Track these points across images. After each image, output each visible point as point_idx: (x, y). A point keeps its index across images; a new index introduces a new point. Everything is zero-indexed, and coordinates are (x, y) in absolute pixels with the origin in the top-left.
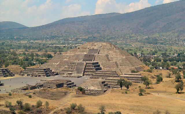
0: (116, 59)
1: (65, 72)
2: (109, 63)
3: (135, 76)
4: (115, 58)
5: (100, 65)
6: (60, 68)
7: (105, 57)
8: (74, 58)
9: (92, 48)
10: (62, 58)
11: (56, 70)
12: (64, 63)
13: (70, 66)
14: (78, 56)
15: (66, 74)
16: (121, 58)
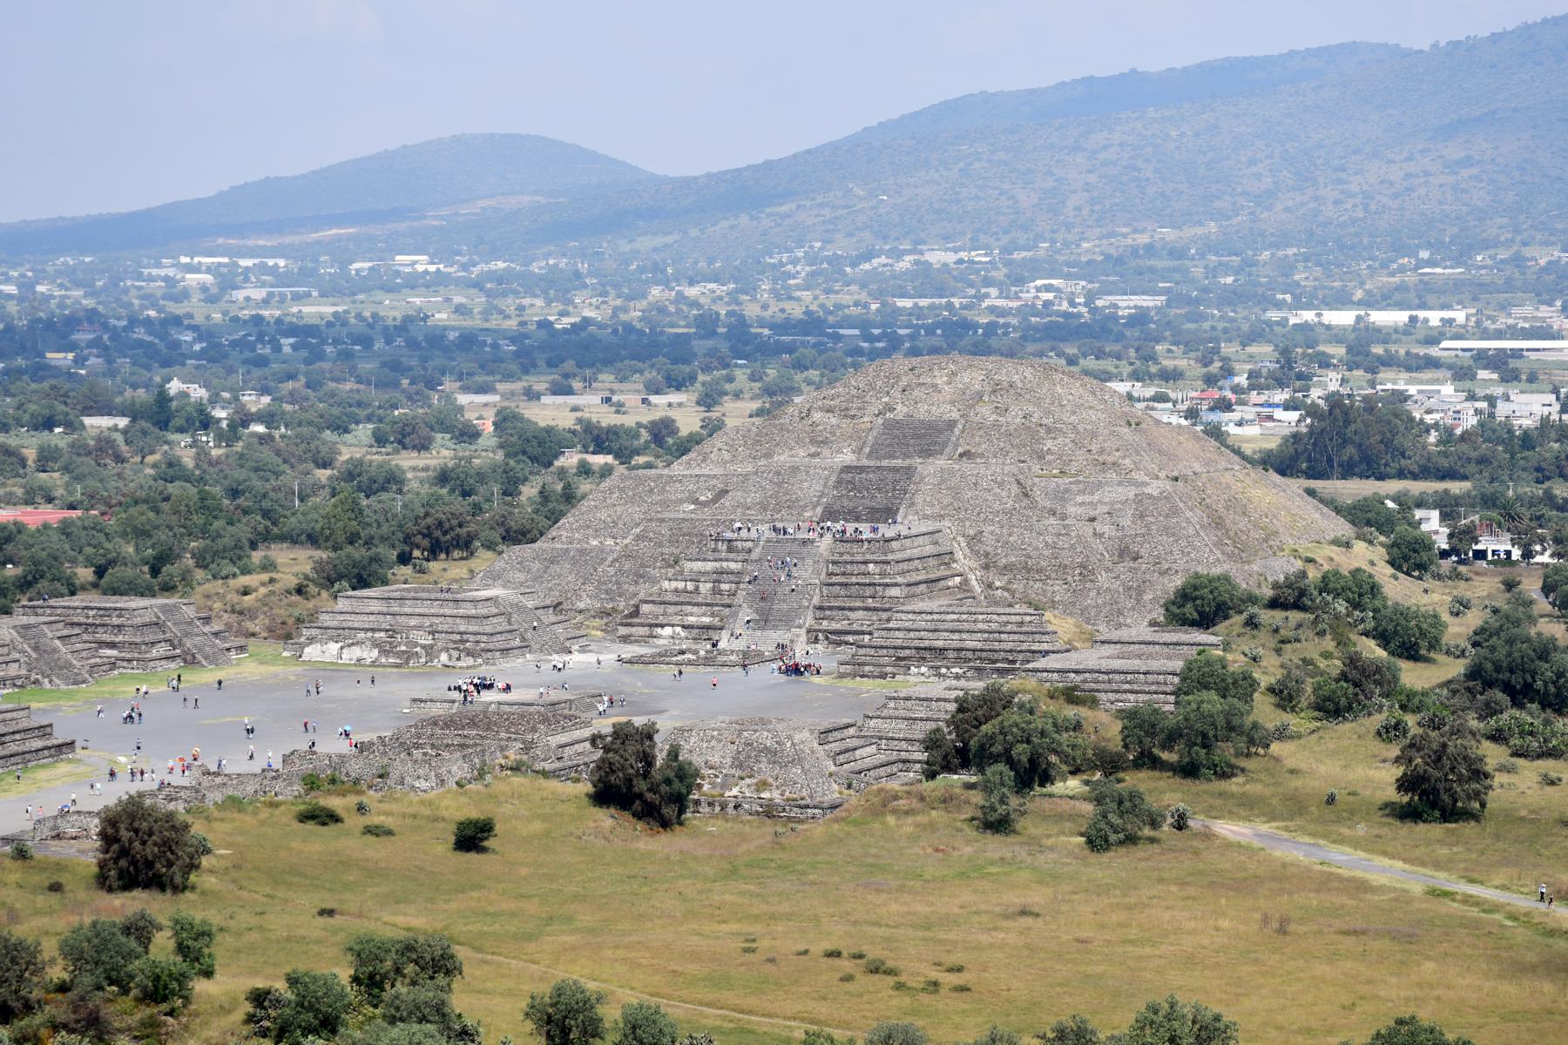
0: (1088, 498)
1: (661, 620)
2: (1027, 534)
3: (1155, 665)
4: (1083, 492)
5: (959, 555)
6: (640, 577)
7: (1001, 485)
8: (754, 497)
9: (901, 411)
10: (656, 498)
11: (612, 599)
12: (673, 541)
13: (710, 566)
14: (783, 477)
15: (668, 631)
16: (1131, 492)
